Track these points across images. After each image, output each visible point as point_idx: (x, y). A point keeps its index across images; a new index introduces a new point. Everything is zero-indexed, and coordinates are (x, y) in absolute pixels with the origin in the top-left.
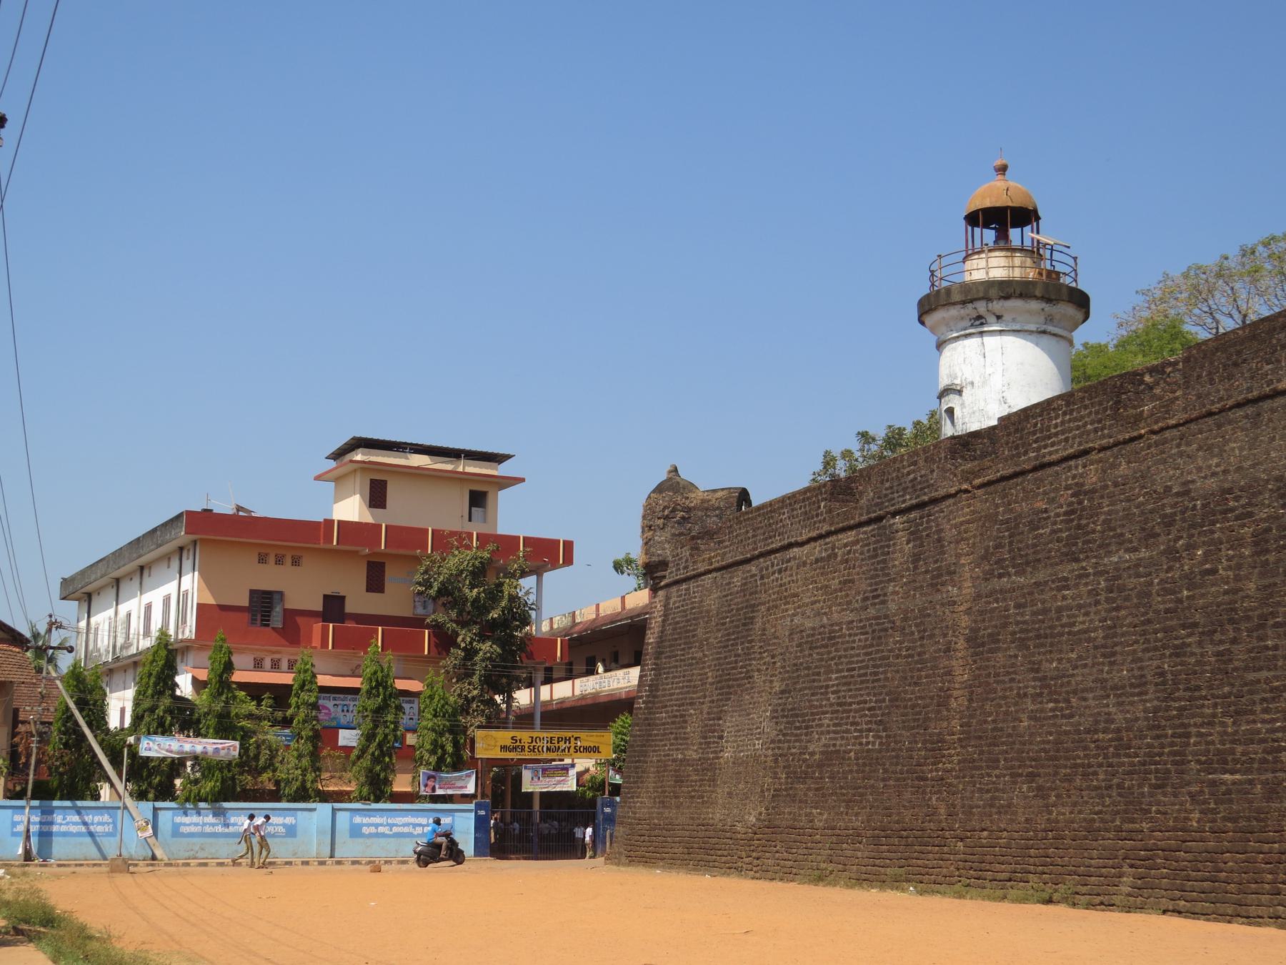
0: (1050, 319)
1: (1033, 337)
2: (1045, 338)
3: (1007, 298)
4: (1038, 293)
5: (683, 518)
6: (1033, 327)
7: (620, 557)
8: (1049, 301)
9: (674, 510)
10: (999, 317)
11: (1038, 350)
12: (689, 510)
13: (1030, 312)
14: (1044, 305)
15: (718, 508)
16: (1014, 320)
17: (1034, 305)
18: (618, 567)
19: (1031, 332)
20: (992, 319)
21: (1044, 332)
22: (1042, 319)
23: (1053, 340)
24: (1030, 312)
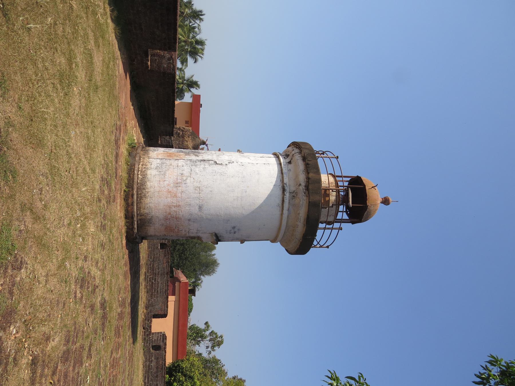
0: (294, 195)
1: (279, 183)
2: (279, 192)
3: (304, 159)
4: (311, 175)
5: (179, 134)
6: (286, 180)
7: (210, 323)
8: (307, 187)
9: (182, 131)
10: (290, 163)
11: (271, 187)
12: (183, 137)
13: (297, 176)
14: (303, 184)
15: (183, 144)
16: (290, 170)
17: (302, 178)
18: (206, 323)
19: (282, 181)
20: (288, 160)
21: (284, 190)
22: (293, 189)
23: (279, 201)
24: (297, 176)
